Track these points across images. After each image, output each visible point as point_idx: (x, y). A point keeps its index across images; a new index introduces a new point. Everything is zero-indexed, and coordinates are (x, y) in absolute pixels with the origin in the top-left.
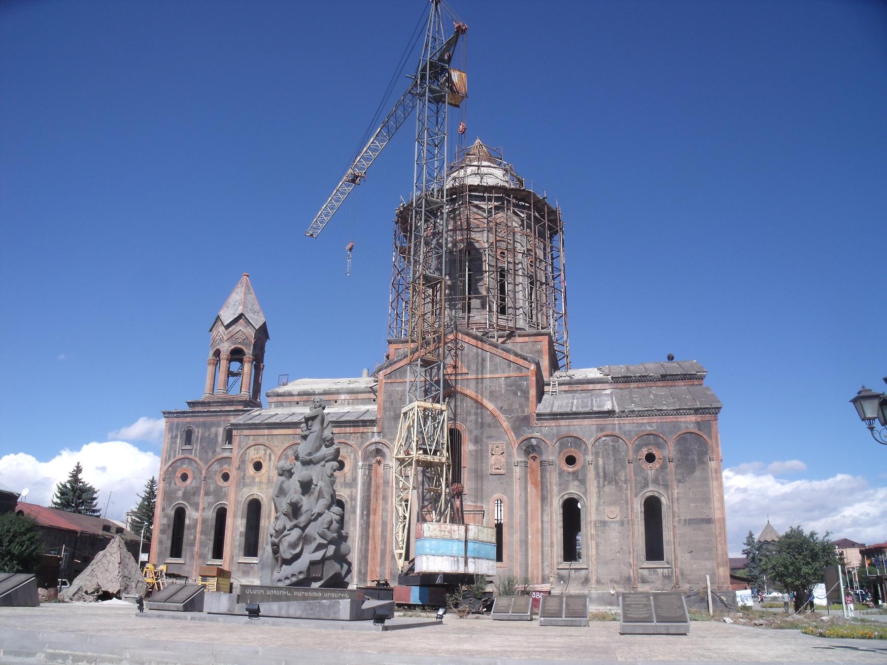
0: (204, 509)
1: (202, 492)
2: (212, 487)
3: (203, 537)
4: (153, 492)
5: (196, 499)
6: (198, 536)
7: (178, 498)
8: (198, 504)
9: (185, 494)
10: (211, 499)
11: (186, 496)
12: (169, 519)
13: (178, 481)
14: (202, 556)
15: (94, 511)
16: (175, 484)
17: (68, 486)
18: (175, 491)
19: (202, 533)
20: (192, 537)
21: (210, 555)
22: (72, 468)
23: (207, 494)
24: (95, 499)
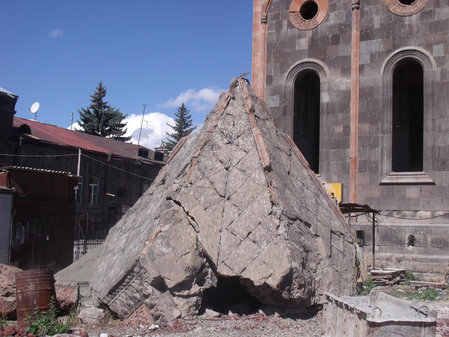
0: (362, 68)
1: (355, 33)
2: (377, 21)
3: (366, 127)
4: (184, 121)
5: (341, 50)
6: (354, 125)
7: (300, 54)
8: (347, 59)
9: (313, 43)
10: (376, 45)
11: (316, 46)
12: (283, 97)
13: (297, 21)
14: (368, 167)
15: (124, 139)
16: (290, 26)
17: (92, 111)
18: (292, 41)
19: (362, 118)
20: (339, 129)
21: (387, 164)
22: (94, 91)
23: (366, 36)
24: (123, 125)
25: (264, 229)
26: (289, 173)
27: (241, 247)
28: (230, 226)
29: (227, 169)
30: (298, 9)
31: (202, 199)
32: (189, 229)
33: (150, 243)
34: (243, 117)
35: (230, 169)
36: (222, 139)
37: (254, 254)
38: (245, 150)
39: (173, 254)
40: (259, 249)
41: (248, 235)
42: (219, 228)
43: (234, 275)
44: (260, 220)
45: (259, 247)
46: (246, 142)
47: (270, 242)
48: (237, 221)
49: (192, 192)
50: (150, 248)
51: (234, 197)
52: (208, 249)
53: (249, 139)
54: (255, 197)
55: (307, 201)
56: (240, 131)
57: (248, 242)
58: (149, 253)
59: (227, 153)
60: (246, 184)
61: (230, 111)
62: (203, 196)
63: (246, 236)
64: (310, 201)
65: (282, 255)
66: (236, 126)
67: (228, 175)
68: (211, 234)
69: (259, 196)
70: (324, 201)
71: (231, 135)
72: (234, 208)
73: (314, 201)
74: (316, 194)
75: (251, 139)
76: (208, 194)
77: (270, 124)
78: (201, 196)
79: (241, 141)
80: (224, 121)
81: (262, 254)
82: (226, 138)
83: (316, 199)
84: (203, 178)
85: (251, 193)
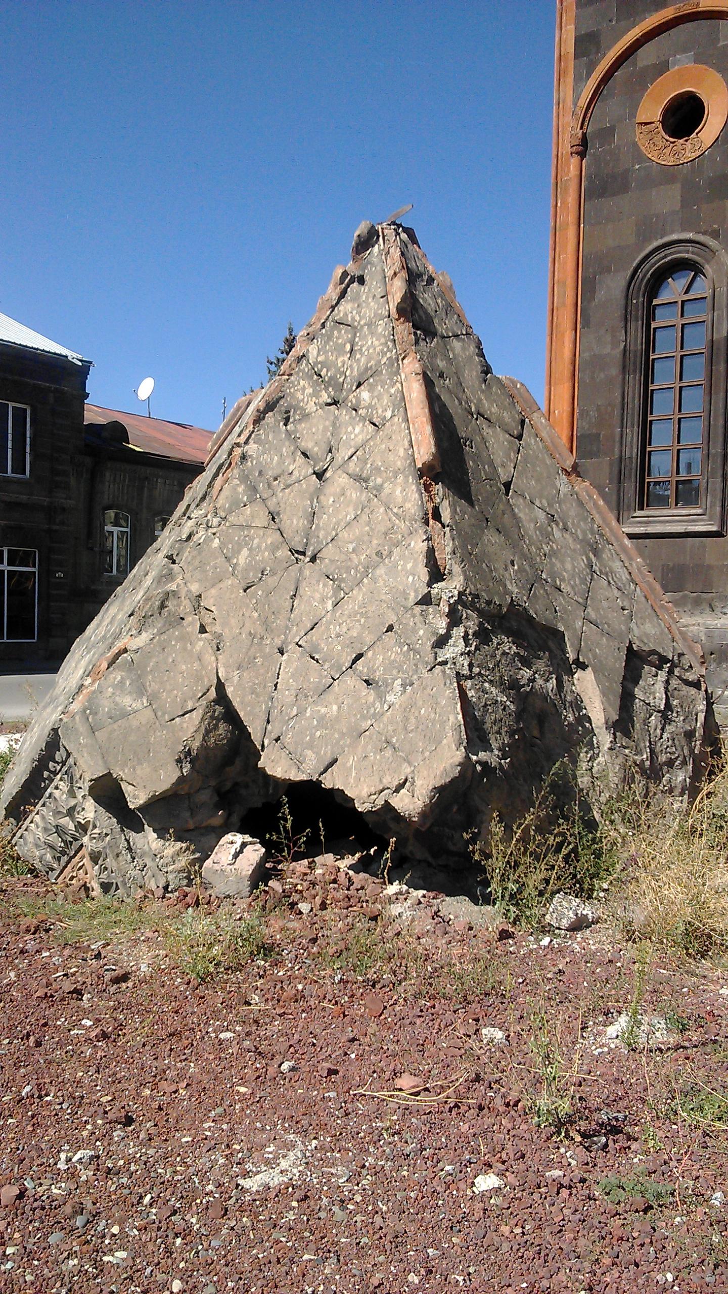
25: (401, 645)
26: (507, 485)
27: (329, 696)
28: (308, 637)
29: (320, 475)
30: (657, 115)
31: (243, 558)
32: (201, 643)
33: (94, 682)
34: (380, 329)
35: (328, 474)
36: (316, 394)
37: (364, 718)
38: (374, 420)
39: (149, 713)
40: (378, 705)
41: (354, 661)
42: (278, 642)
43: (304, 777)
44: (392, 619)
45: (381, 697)
46: (379, 398)
47: (412, 684)
48: (329, 623)
49: (217, 540)
50: (91, 698)
51: (328, 553)
52: (242, 702)
53: (387, 391)
54: (385, 553)
55: (558, 565)
56: (367, 369)
57: (351, 682)
58: (85, 711)
59: (325, 429)
60: (365, 518)
61: (346, 315)
62: (245, 552)
63: (348, 665)
64: (569, 566)
65: (443, 723)
66: (358, 356)
67: (317, 494)
68: (255, 658)
69: (396, 551)
70: (617, 565)
71: (341, 380)
72: (324, 585)
73: (582, 562)
74: (591, 546)
75: (393, 391)
76: (259, 547)
77: (464, 349)
78: (239, 552)
79: (365, 394)
80: (327, 343)
81: (385, 719)
82: (326, 389)
83: (588, 559)
84: (252, 501)
85: (375, 542)
